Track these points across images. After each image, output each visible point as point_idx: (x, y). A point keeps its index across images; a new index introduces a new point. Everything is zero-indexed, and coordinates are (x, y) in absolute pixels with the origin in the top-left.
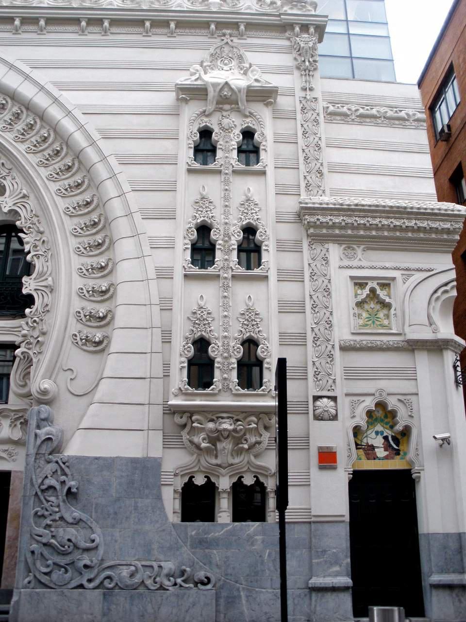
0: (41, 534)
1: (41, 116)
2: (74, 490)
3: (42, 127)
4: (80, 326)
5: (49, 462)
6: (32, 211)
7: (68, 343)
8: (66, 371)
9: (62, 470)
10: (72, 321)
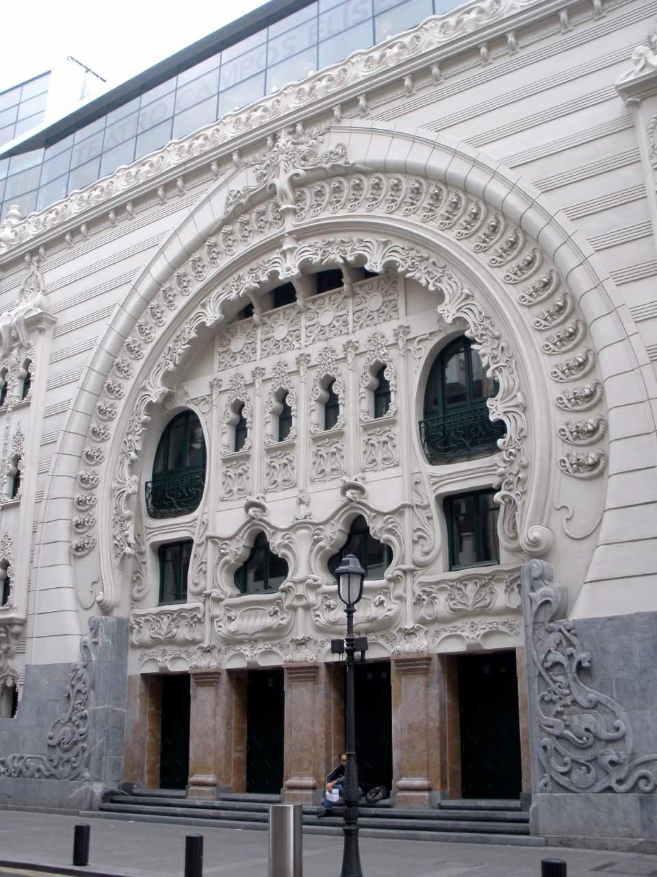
0: (552, 724)
1: (464, 188)
2: (586, 664)
3: (469, 201)
4: (568, 448)
5: (550, 631)
6: (480, 313)
7: (556, 473)
8: (558, 510)
9: (568, 640)
10: (557, 443)
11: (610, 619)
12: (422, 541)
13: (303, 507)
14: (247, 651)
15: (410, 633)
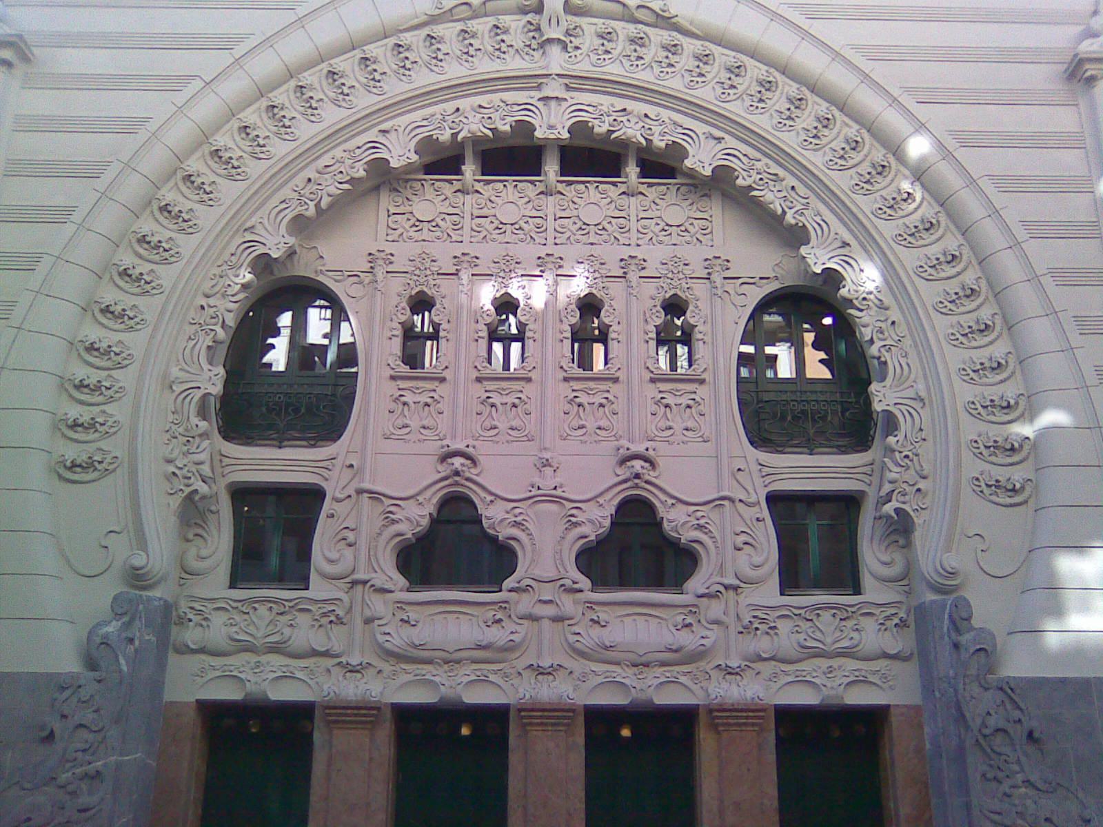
0: (999, 810)
10: (967, 456)
11: (1063, 681)
12: (747, 548)
13: (548, 471)
14: (439, 675)
15: (730, 672)
